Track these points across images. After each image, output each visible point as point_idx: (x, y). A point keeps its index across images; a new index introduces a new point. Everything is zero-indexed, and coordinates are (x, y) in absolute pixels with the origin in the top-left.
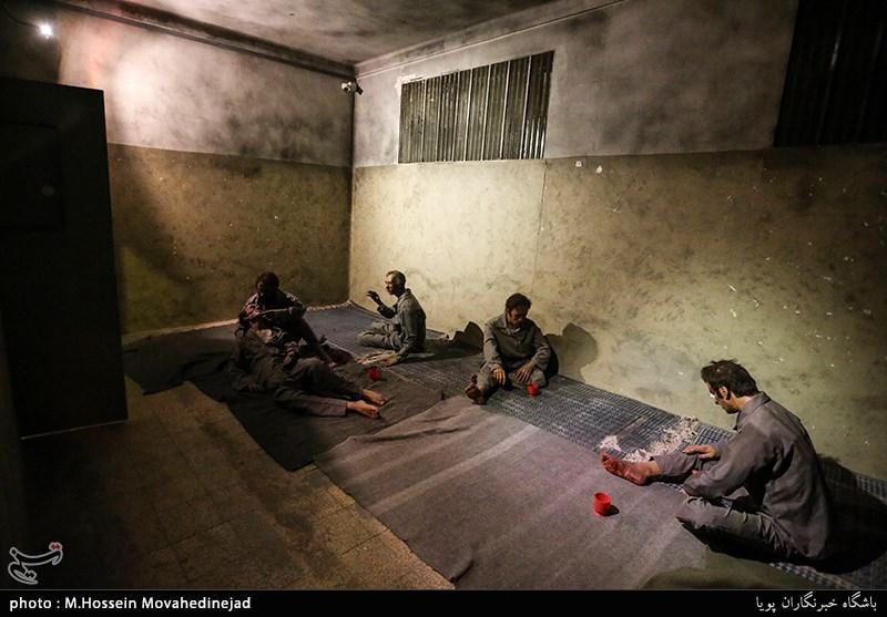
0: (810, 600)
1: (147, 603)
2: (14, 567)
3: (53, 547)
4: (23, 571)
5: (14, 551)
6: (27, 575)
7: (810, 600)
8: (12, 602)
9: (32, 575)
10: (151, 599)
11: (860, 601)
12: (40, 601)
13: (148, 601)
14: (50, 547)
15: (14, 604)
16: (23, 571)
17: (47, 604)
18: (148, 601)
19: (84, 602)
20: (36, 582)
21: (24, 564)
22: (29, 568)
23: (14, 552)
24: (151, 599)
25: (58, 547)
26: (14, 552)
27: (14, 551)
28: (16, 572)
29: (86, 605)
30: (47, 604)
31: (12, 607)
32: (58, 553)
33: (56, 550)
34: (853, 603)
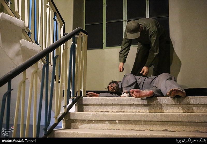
0: (189, 140)
2: (3, 132)
3: (12, 128)
5: (3, 129)
6: (6, 134)
7: (189, 140)
8: (2, 140)
9: (7, 134)
11: (202, 140)
12: (8, 140)
14: (11, 128)
15: (3, 141)
16: (5, 133)
20: (8, 136)
21: (5, 132)
22: (7, 133)
23: (3, 129)
26: (3, 129)
28: (3, 133)
31: (2, 142)
33: (13, 128)
34: (200, 141)
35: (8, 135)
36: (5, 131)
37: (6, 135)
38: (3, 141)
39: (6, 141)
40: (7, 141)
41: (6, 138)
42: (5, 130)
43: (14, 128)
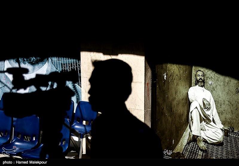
1: (31, 162)
3: (14, 147)
5: (3, 148)
6: (7, 155)
10: (32, 161)
13: (31, 161)
14: (13, 147)
17: (11, 163)
18: (31, 161)
19: (16, 162)
21: (5, 152)
23: (3, 148)
24: (32, 161)
25: (15, 147)
26: (3, 148)
27: (3, 148)
29: (17, 163)
30: (10, 162)
31: (3, 163)
33: (15, 148)
36: (5, 151)
38: (4, 163)
39: (7, 163)
40: (8, 163)
42: (6, 150)
43: (16, 148)
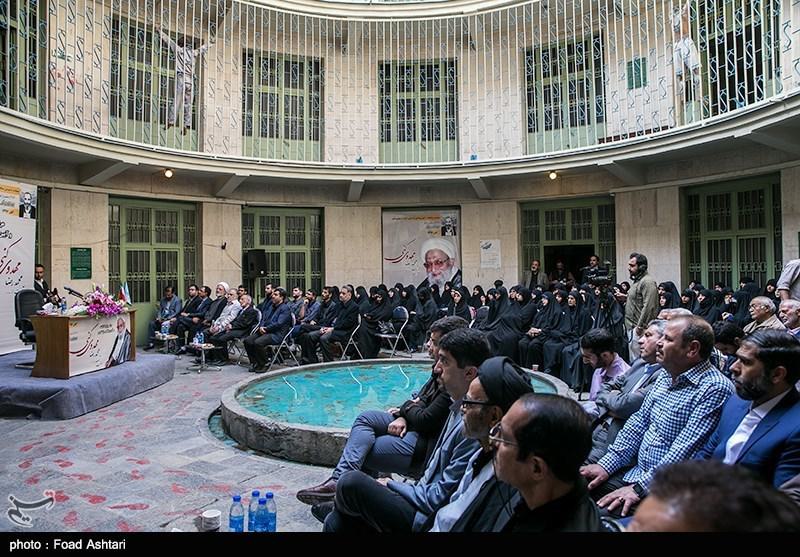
2: (11, 512)
3: (47, 493)
4: (20, 515)
6: (24, 519)
9: (28, 519)
16: (20, 515)
17: (38, 545)
23: (11, 498)
26: (11, 498)
28: (13, 516)
31: (11, 548)
32: (51, 499)
33: (50, 496)
35: (32, 522)
37: (22, 522)
38: (14, 545)
40: (27, 545)
41: (25, 536)
42: (18, 504)
